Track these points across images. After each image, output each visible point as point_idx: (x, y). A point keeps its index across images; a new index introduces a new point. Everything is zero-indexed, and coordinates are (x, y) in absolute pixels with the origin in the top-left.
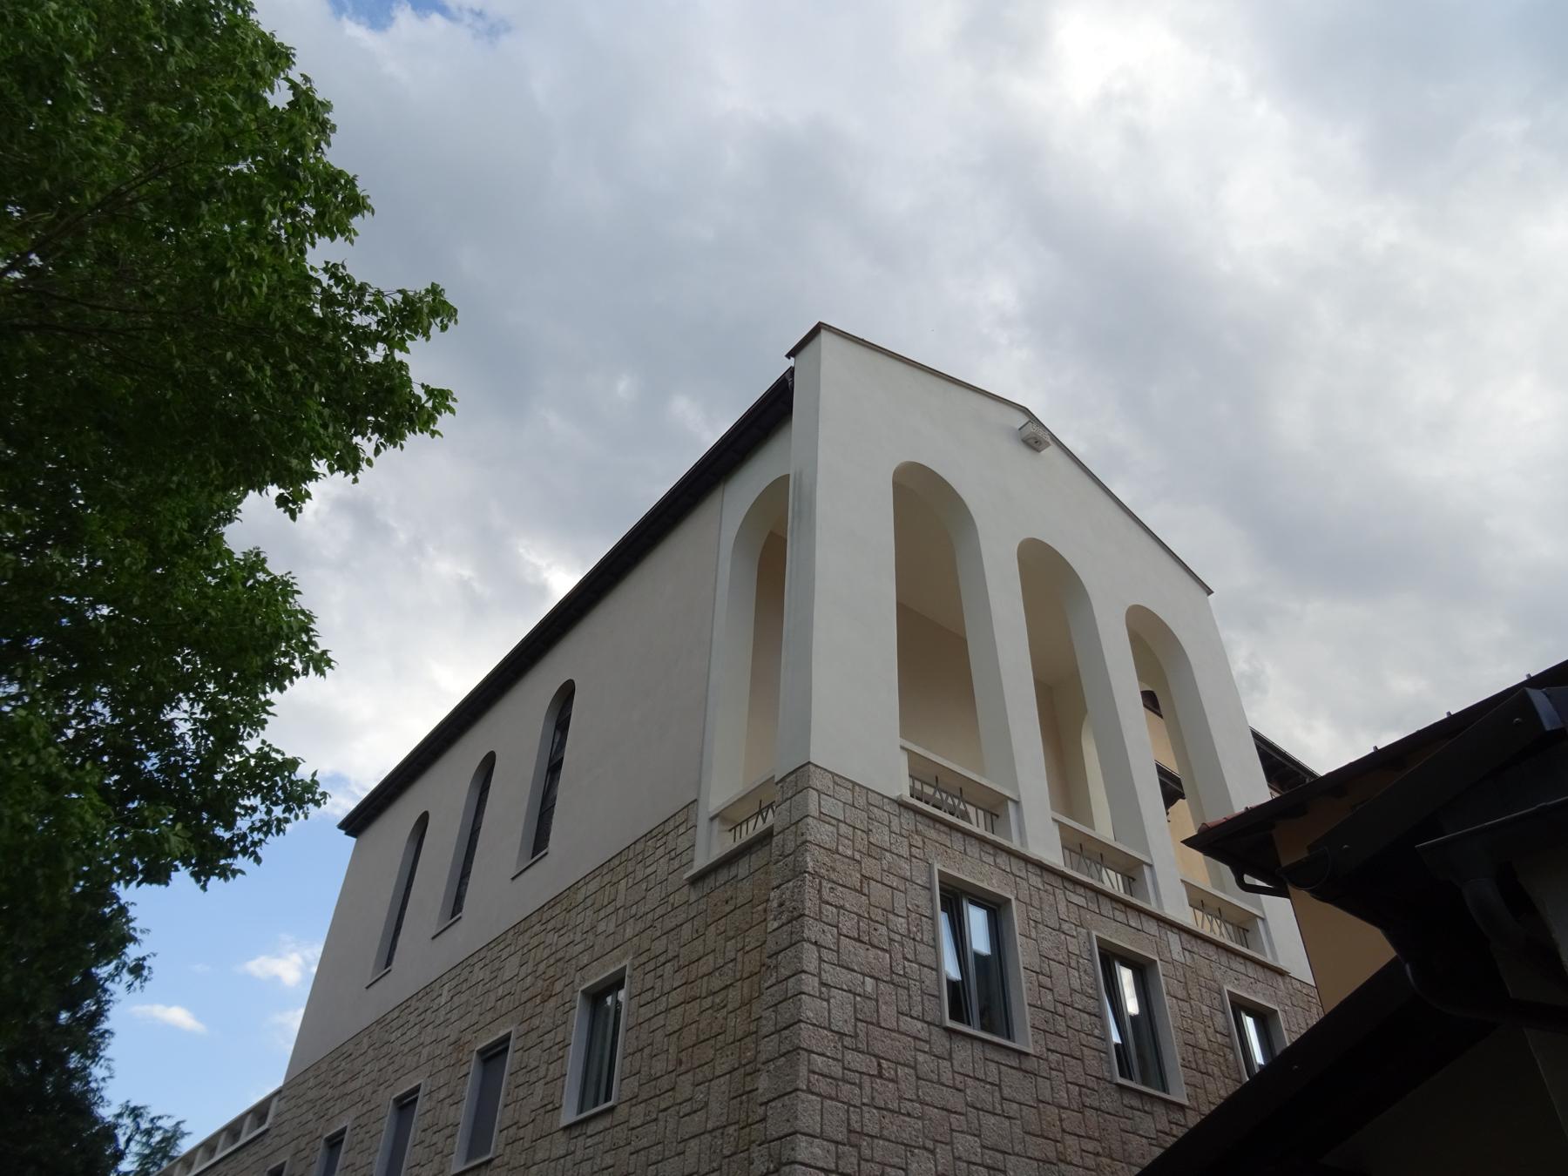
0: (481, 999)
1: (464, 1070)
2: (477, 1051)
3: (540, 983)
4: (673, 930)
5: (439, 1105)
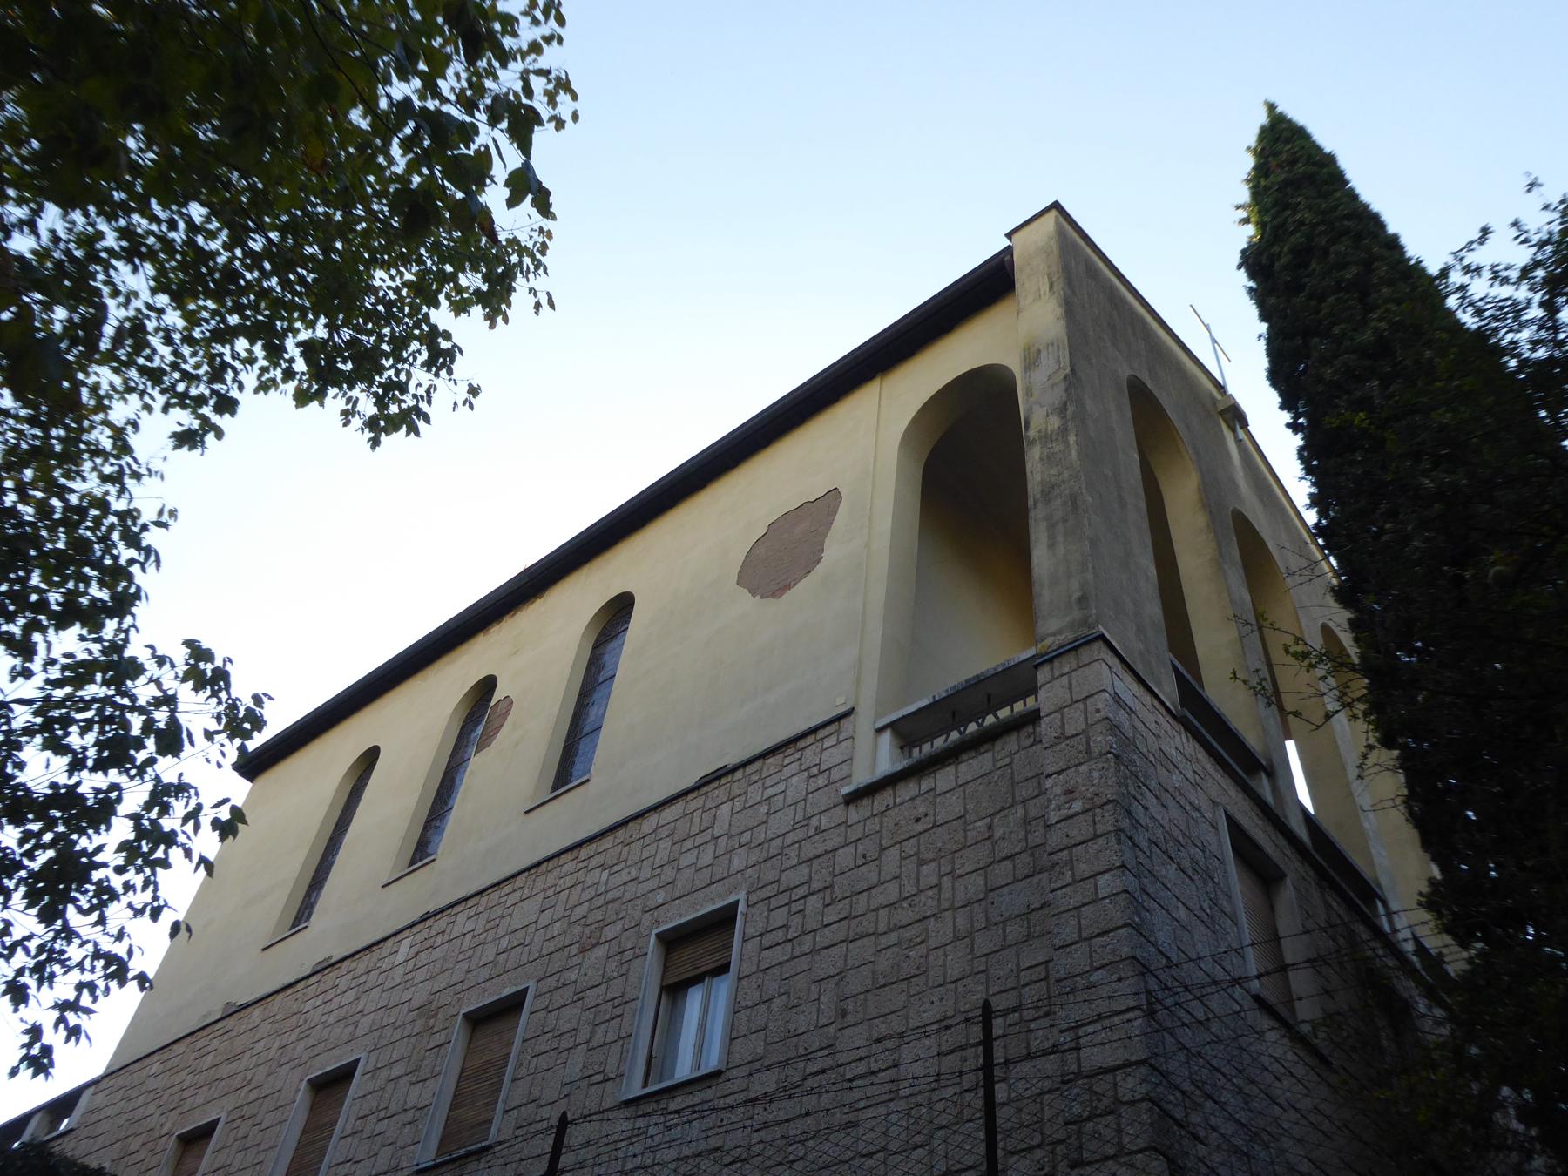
0: (470, 953)
1: (439, 1038)
2: (178, 1136)
3: (577, 929)
4: (819, 856)
5: (391, 1086)
